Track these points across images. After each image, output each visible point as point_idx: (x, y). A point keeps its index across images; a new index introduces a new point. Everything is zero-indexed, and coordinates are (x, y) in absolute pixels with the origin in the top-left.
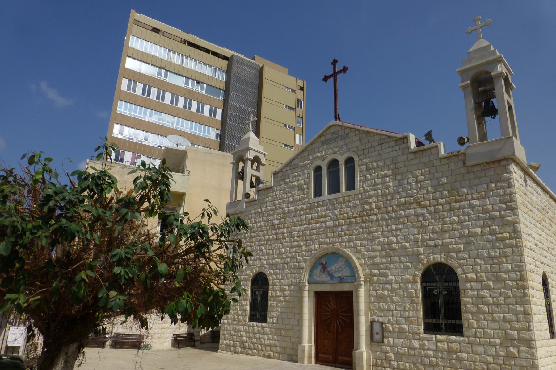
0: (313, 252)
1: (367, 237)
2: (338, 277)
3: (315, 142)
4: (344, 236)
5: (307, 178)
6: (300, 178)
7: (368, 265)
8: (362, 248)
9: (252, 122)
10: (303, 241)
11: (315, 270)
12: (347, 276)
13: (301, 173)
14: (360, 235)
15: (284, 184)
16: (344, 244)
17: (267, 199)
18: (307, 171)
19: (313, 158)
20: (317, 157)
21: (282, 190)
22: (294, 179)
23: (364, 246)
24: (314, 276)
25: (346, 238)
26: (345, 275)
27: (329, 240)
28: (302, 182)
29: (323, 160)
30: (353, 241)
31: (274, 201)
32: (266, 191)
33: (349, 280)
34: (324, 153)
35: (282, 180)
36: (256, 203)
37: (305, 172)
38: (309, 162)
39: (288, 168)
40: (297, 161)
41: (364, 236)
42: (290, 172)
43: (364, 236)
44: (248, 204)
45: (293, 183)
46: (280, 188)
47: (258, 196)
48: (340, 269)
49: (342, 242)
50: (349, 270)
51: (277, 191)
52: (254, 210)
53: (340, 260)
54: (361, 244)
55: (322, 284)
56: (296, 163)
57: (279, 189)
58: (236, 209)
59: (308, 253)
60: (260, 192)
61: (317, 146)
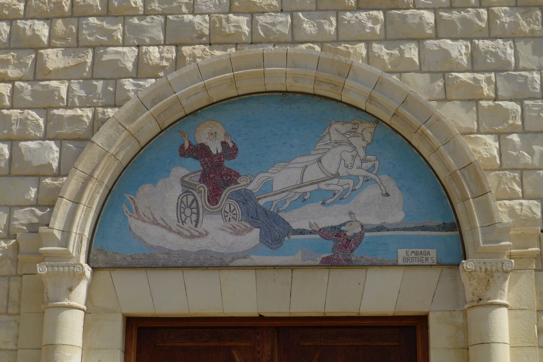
0: (128, 84)
1: (516, 24)
2: (324, 233)
4: (351, 10)
7: (523, 170)
8: (481, 76)
10: (49, 19)
11: (147, 188)
12: (380, 228)
14: (464, 8)
16: (362, 48)
23: (496, 71)
24: (135, 223)
25: (375, 20)
26: (375, 221)
27: (252, 24)
30: (419, 40)
33: (402, 253)
41: (492, 18)
43: (492, 18)
48: (334, 185)
49: (338, 41)
50: (397, 196)
53: (335, 136)
54: (472, 57)
55: (192, 276)
59: (90, 90)
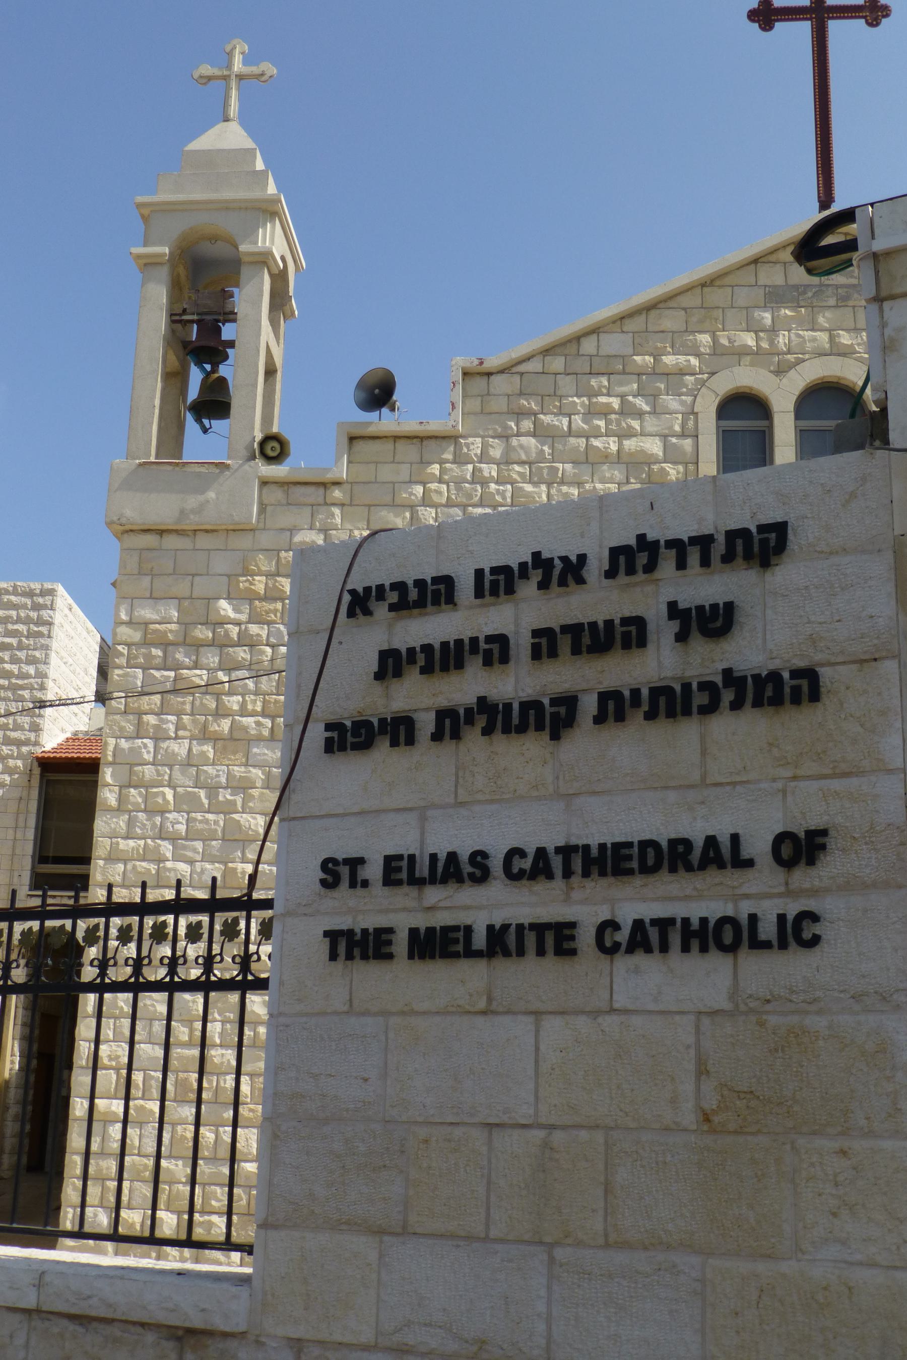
3: (727, 280)
5: (683, 435)
6: (636, 424)
9: (240, 77)
13: (641, 403)
15: (534, 435)
17: (419, 490)
18: (683, 403)
19: (717, 350)
20: (742, 352)
21: (522, 463)
22: (602, 423)
28: (654, 447)
29: (780, 371)
31: (464, 507)
32: (408, 451)
34: (782, 340)
35: (520, 414)
36: (337, 494)
37: (671, 402)
38: (694, 361)
39: (557, 363)
40: (613, 344)
42: (566, 384)
44: (276, 495)
45: (596, 443)
46: (508, 449)
47: (349, 462)
51: (484, 457)
52: (325, 531)
56: (605, 350)
57: (496, 452)
58: (192, 501)
60: (360, 446)
61: (741, 302)
